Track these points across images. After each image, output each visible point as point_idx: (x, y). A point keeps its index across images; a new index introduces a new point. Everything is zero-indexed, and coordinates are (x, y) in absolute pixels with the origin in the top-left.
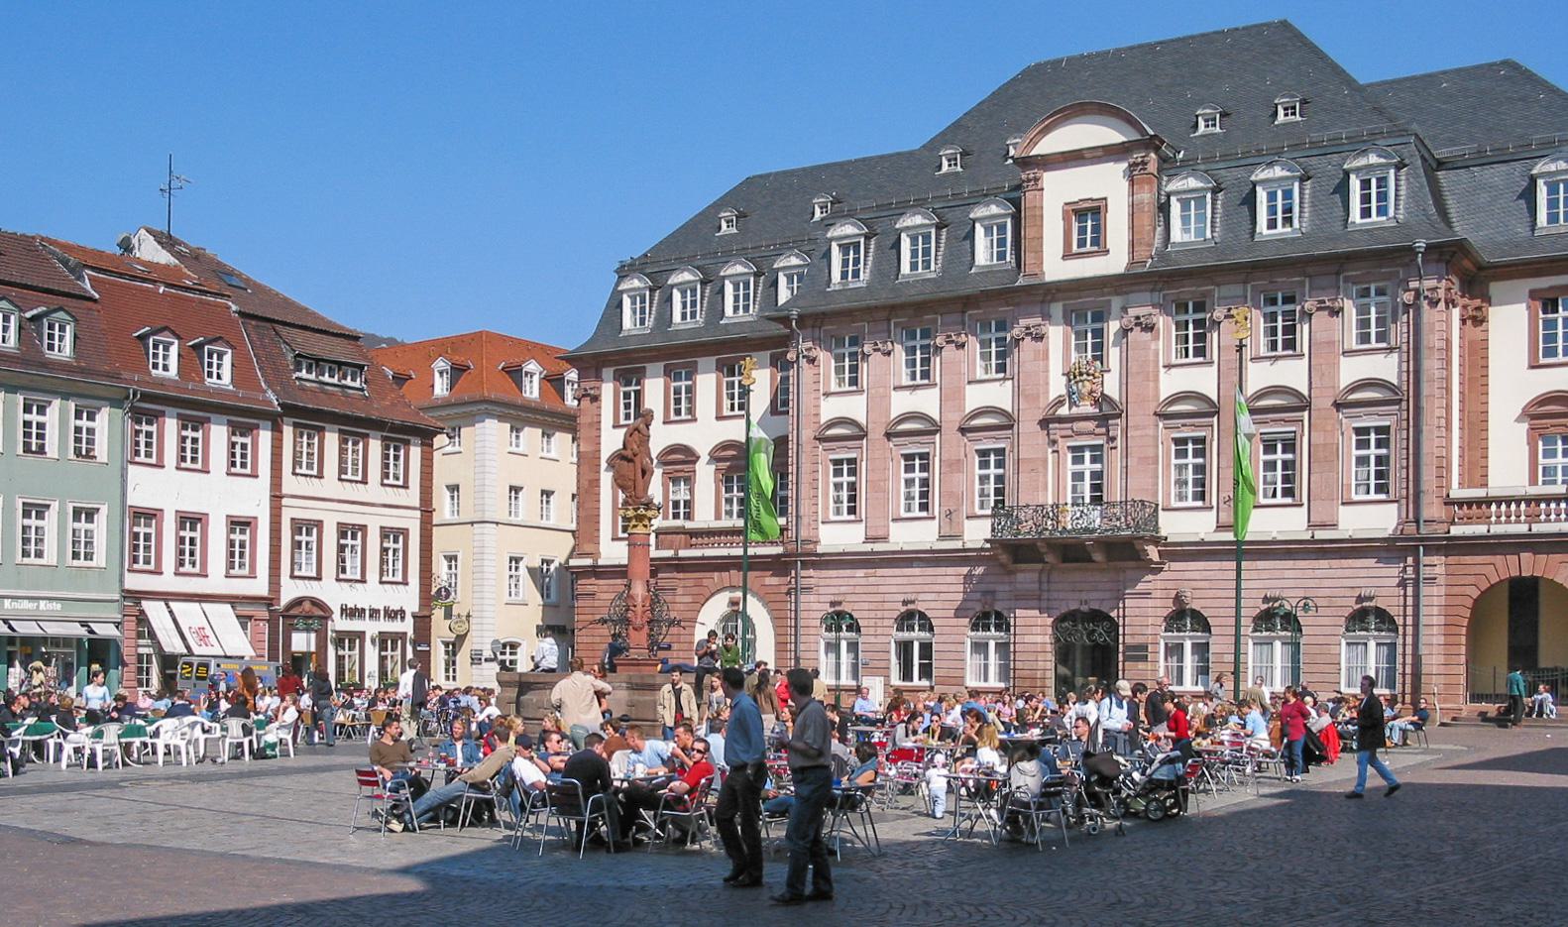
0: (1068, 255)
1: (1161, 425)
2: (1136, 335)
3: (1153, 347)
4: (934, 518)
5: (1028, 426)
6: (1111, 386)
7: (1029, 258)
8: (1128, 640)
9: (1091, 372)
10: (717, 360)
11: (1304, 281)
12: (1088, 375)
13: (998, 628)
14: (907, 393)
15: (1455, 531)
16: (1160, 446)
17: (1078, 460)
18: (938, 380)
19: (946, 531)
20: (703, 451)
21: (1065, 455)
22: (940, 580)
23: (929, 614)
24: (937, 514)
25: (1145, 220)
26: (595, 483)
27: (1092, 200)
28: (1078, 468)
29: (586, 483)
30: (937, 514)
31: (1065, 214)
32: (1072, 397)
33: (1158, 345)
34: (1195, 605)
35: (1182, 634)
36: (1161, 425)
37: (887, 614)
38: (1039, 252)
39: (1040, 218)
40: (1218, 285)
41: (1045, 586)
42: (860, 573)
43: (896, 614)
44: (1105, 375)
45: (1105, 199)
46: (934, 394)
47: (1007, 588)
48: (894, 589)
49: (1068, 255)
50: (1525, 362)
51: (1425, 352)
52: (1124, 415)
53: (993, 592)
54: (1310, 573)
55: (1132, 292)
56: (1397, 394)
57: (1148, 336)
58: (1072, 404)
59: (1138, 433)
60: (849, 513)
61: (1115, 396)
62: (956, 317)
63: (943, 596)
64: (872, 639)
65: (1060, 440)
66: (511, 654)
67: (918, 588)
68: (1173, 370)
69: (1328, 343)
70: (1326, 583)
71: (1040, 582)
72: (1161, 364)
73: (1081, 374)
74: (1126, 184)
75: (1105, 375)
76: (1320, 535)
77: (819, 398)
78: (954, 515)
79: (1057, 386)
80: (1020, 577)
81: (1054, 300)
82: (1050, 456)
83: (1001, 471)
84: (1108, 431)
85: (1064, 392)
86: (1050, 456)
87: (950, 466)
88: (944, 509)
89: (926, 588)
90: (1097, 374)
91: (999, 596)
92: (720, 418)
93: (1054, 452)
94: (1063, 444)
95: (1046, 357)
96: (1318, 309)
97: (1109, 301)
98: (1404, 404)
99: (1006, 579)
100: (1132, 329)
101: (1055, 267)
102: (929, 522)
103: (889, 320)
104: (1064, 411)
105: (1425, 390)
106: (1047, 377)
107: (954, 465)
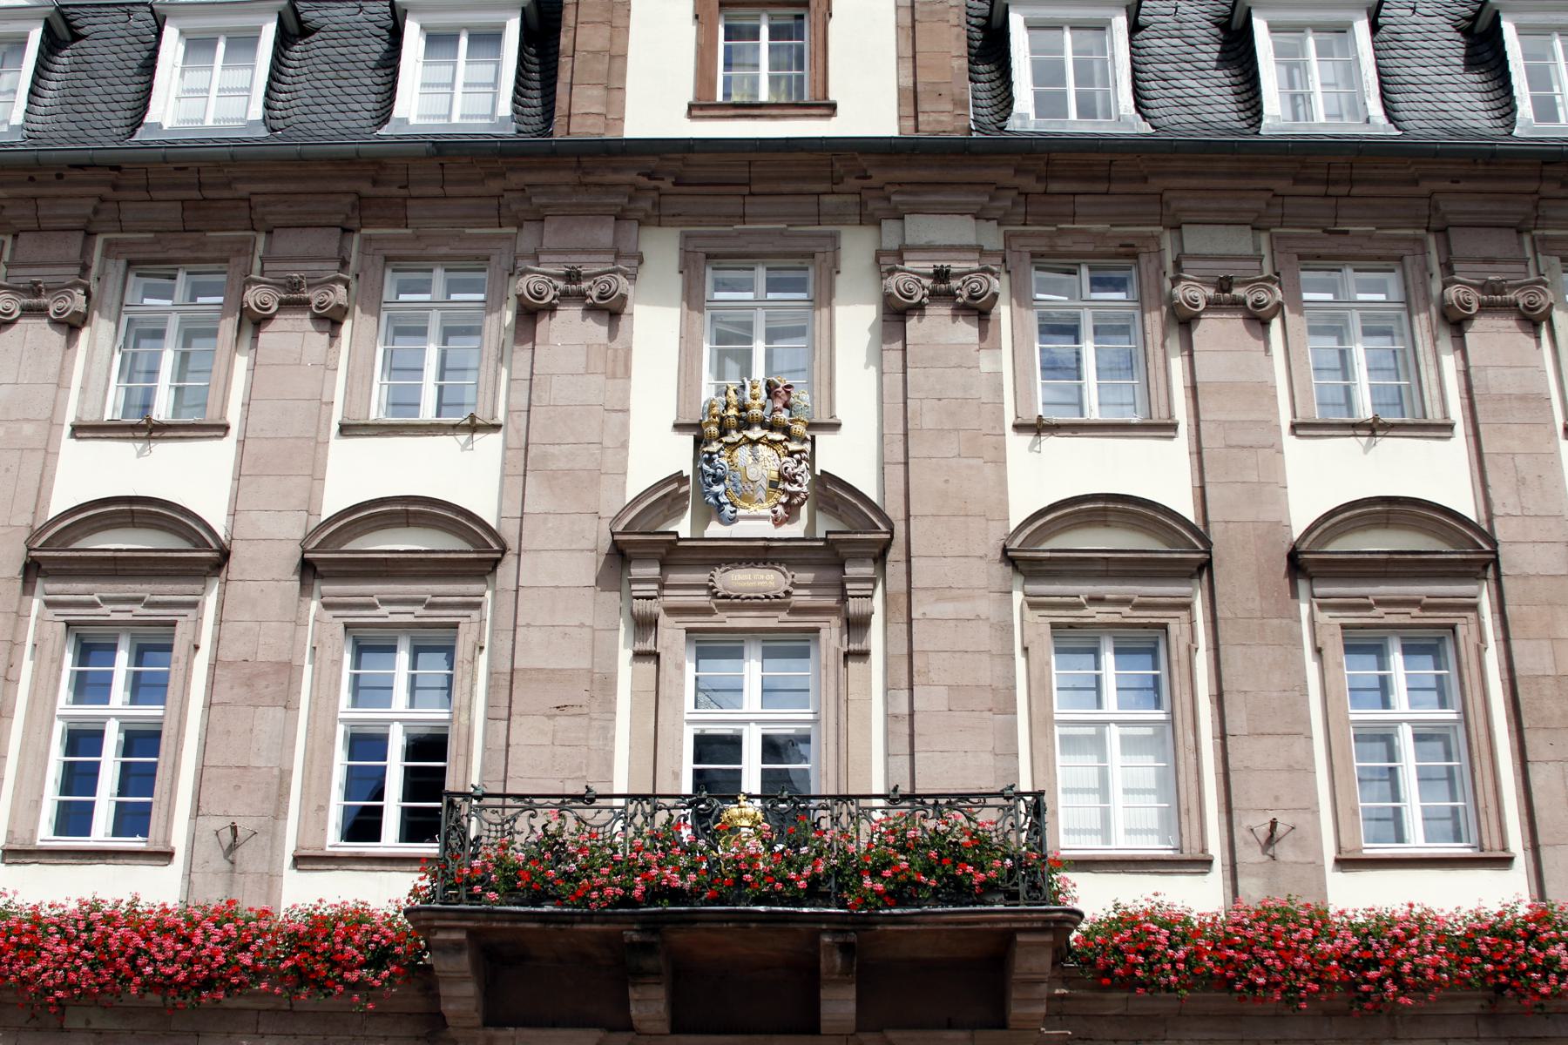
1: (1018, 597)
4: (166, 856)
9: (784, 416)
11: (1421, 241)
12: (772, 427)
16: (1020, 661)
21: (680, 667)
24: (179, 842)
33: (999, 361)
36: (1018, 597)
44: (823, 439)
52: (895, 553)
57: (966, 331)
58: (715, 511)
59: (947, 609)
62: (327, 241)
65: (664, 620)
68: (1050, 442)
69: (1523, 398)
73: (745, 423)
75: (823, 439)
78: (242, 854)
81: (656, 219)
84: (844, 598)
85: (688, 471)
87: (249, 682)
90: (799, 428)
93: (639, 656)
94: (671, 634)
95: (620, 367)
96: (1487, 308)
97: (834, 238)
100: (920, 307)
103: (89, 235)
106: (625, 427)
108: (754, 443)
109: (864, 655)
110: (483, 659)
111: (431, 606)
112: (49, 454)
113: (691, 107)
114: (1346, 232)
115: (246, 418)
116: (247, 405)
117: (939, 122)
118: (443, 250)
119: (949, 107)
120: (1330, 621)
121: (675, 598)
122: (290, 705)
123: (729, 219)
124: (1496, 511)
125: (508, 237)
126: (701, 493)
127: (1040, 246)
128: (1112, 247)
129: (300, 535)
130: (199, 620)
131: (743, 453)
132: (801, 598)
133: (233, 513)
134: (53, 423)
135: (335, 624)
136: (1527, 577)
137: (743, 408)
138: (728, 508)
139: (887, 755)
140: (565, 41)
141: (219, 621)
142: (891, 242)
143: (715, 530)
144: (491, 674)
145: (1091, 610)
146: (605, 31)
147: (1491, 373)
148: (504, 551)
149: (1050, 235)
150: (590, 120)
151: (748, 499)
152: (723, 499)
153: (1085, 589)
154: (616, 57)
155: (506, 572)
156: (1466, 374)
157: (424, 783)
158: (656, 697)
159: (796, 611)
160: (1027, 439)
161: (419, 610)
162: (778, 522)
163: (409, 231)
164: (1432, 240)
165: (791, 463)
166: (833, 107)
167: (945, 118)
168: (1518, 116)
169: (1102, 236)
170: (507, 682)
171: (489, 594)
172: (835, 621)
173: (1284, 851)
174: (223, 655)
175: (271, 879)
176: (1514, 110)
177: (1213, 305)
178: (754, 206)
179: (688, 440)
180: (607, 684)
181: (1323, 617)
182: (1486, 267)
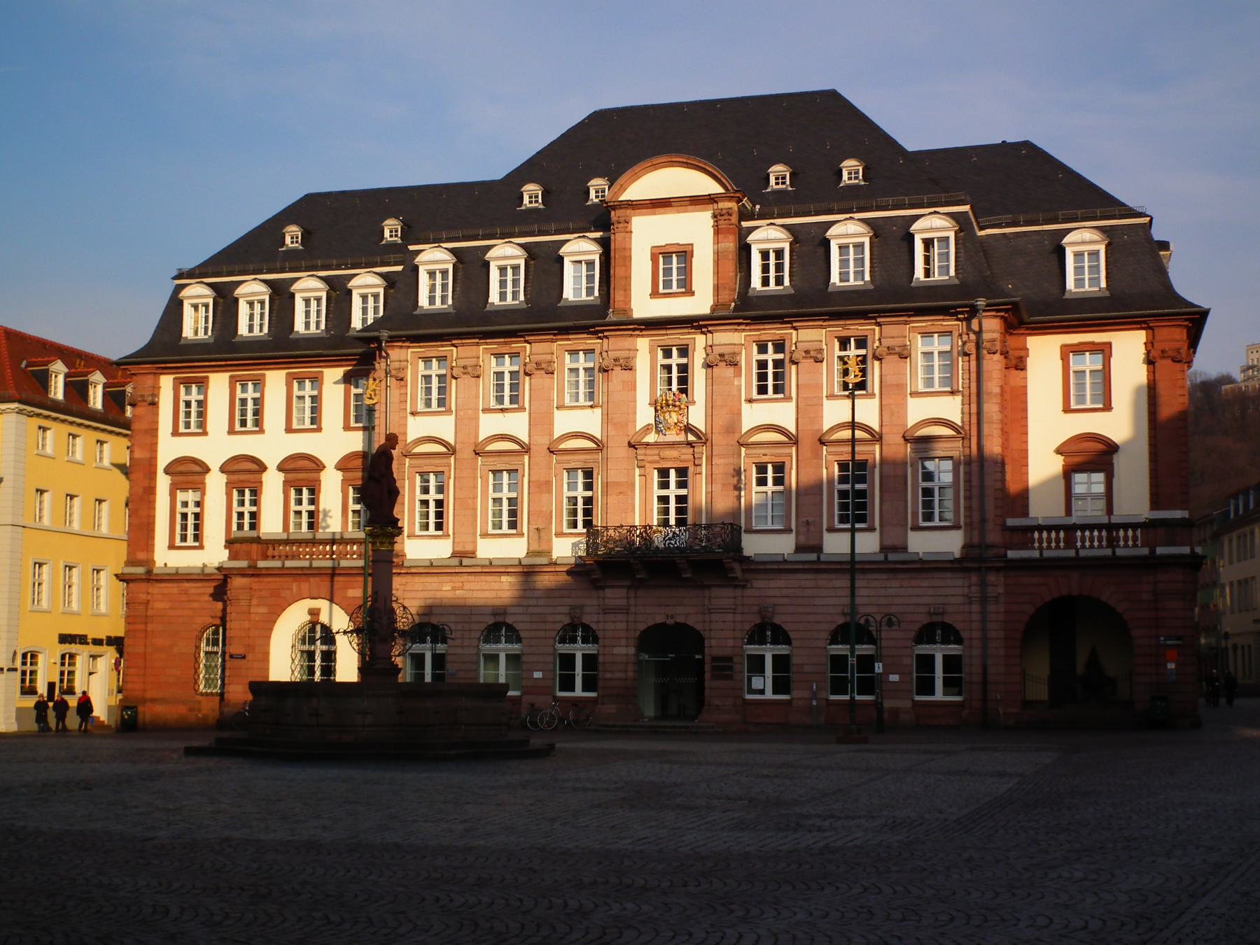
0: (655, 294)
2: (724, 371)
3: (736, 383)
5: (618, 450)
6: (697, 416)
7: (617, 296)
8: (717, 652)
10: (287, 374)
12: (674, 406)
13: (585, 641)
14: (501, 415)
15: (1011, 554)
17: (664, 485)
18: (527, 405)
19: (535, 547)
20: (272, 461)
21: (652, 479)
23: (518, 626)
25: (730, 266)
26: (151, 490)
27: (678, 244)
28: (664, 492)
29: (141, 490)
30: (525, 530)
31: (654, 259)
32: (658, 427)
33: (741, 382)
34: (777, 620)
35: (764, 646)
36: (743, 454)
37: (475, 626)
38: (627, 289)
39: (627, 260)
40: (795, 328)
41: (632, 601)
42: (447, 587)
43: (483, 626)
45: (692, 245)
46: (523, 417)
47: (595, 602)
49: (655, 294)
50: (1060, 406)
51: (985, 397)
53: (582, 607)
55: (717, 331)
56: (961, 433)
57: (731, 370)
60: (436, 529)
61: (701, 427)
64: (459, 651)
65: (647, 465)
66: (69, 665)
68: (754, 405)
69: (897, 385)
71: (628, 598)
72: (743, 398)
74: (711, 231)
76: (892, 557)
77: (406, 417)
78: (542, 534)
79: (645, 415)
80: (608, 592)
82: (637, 479)
83: (589, 494)
86: (637, 479)
88: (533, 527)
90: (682, 406)
91: (588, 610)
92: (289, 430)
95: (633, 387)
101: (643, 305)
102: (517, 540)
104: (651, 438)
105: (986, 429)
106: (635, 407)
107: (541, 487)
108: (670, 412)
109: (701, 473)
112: (477, 419)
113: (650, 295)
114: (850, 329)
115: (530, 406)
116: (530, 401)
117: (724, 298)
119: (728, 292)
121: (650, 458)
122: (550, 492)
123: (663, 335)
124: (884, 424)
126: (656, 427)
127: (756, 338)
129: (548, 443)
131: (667, 414)
133: (530, 436)
134: (477, 409)
136: (890, 444)
137: (667, 400)
138: (664, 431)
140: (612, 272)
141: (529, 469)
142: (710, 343)
143: (662, 439)
146: (623, 268)
147: (888, 377)
148: (603, 447)
150: (621, 303)
151: (669, 428)
152: (662, 428)
153: (763, 451)
154: (628, 278)
157: (588, 512)
158: (646, 488)
159: (681, 461)
160: (749, 405)
162: (677, 434)
164: (877, 329)
165: (680, 417)
166: (692, 294)
167: (727, 297)
168: (915, 276)
170: (606, 485)
173: (812, 528)
175: (550, 541)
176: (913, 273)
179: (653, 409)
180: (633, 485)
181: (830, 458)
182: (891, 339)
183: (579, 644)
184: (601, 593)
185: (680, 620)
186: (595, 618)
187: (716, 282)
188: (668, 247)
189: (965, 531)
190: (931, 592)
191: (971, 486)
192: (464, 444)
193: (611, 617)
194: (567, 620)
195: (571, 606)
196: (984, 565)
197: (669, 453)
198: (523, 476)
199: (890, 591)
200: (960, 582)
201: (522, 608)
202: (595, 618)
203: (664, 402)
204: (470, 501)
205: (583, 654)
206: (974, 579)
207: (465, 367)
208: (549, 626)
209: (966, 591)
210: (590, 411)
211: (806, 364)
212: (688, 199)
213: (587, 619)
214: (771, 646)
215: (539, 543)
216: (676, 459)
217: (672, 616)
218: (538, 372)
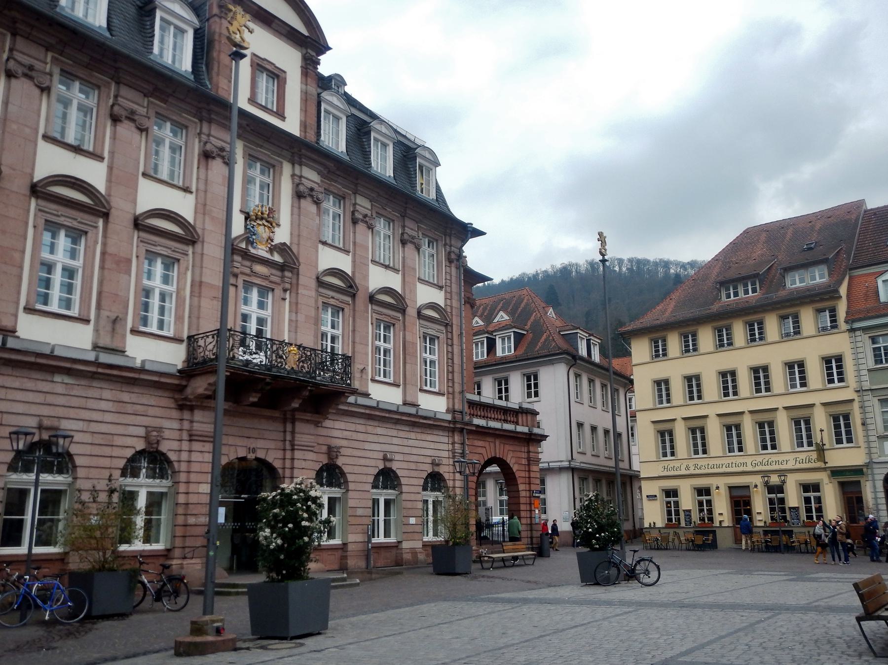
2: (308, 205)
12: (268, 222)
19: (106, 341)
22: (92, 404)
48: (20, 408)
53: (160, 429)
54: (405, 442)
63: (95, 427)
65: (240, 276)
67: (60, 412)
70: (415, 451)
73: (262, 219)
87: (118, 263)
89: (72, 413)
91: (167, 434)
98: (449, 329)
99: (175, 414)
102: (79, 326)
110: (189, 274)
111: (174, 251)
118: (174, 118)
120: (375, 316)
123: (258, 145)
125: (195, 123)
128: (341, 193)
130: (97, 234)
132: (273, 278)
135: (143, 248)
137: (262, 213)
139: (289, 331)
144: (193, 281)
145: (332, 300)
149: (329, 185)
153: (331, 293)
155: (198, 246)
156: (404, 258)
159: (271, 282)
161: (169, 251)
163: (165, 106)
169: (339, 189)
171: (190, 252)
172: (280, 288)
174: (111, 249)
175: (124, 337)
177: (362, 221)
178: (266, 145)
183: (142, 479)
184: (186, 415)
185: (261, 455)
186: (175, 445)
187: (303, 119)
188: (265, 62)
189: (448, 398)
190: (432, 445)
191: (453, 363)
192: (14, 170)
193: (197, 446)
194: (140, 445)
195: (146, 427)
196: (466, 427)
197: (259, 269)
198: (96, 242)
199: (411, 443)
200: (445, 440)
201: (81, 423)
202: (175, 445)
203: (260, 213)
204: (17, 255)
205: (148, 492)
206: (457, 438)
207: (31, 68)
208: (116, 452)
209: (450, 447)
210: (181, 194)
211: (361, 227)
212: (288, 29)
213: (164, 447)
214: (328, 488)
215: (113, 337)
216: (265, 278)
217: (254, 450)
218: (126, 122)
